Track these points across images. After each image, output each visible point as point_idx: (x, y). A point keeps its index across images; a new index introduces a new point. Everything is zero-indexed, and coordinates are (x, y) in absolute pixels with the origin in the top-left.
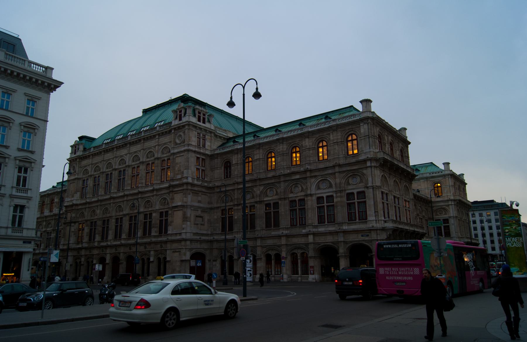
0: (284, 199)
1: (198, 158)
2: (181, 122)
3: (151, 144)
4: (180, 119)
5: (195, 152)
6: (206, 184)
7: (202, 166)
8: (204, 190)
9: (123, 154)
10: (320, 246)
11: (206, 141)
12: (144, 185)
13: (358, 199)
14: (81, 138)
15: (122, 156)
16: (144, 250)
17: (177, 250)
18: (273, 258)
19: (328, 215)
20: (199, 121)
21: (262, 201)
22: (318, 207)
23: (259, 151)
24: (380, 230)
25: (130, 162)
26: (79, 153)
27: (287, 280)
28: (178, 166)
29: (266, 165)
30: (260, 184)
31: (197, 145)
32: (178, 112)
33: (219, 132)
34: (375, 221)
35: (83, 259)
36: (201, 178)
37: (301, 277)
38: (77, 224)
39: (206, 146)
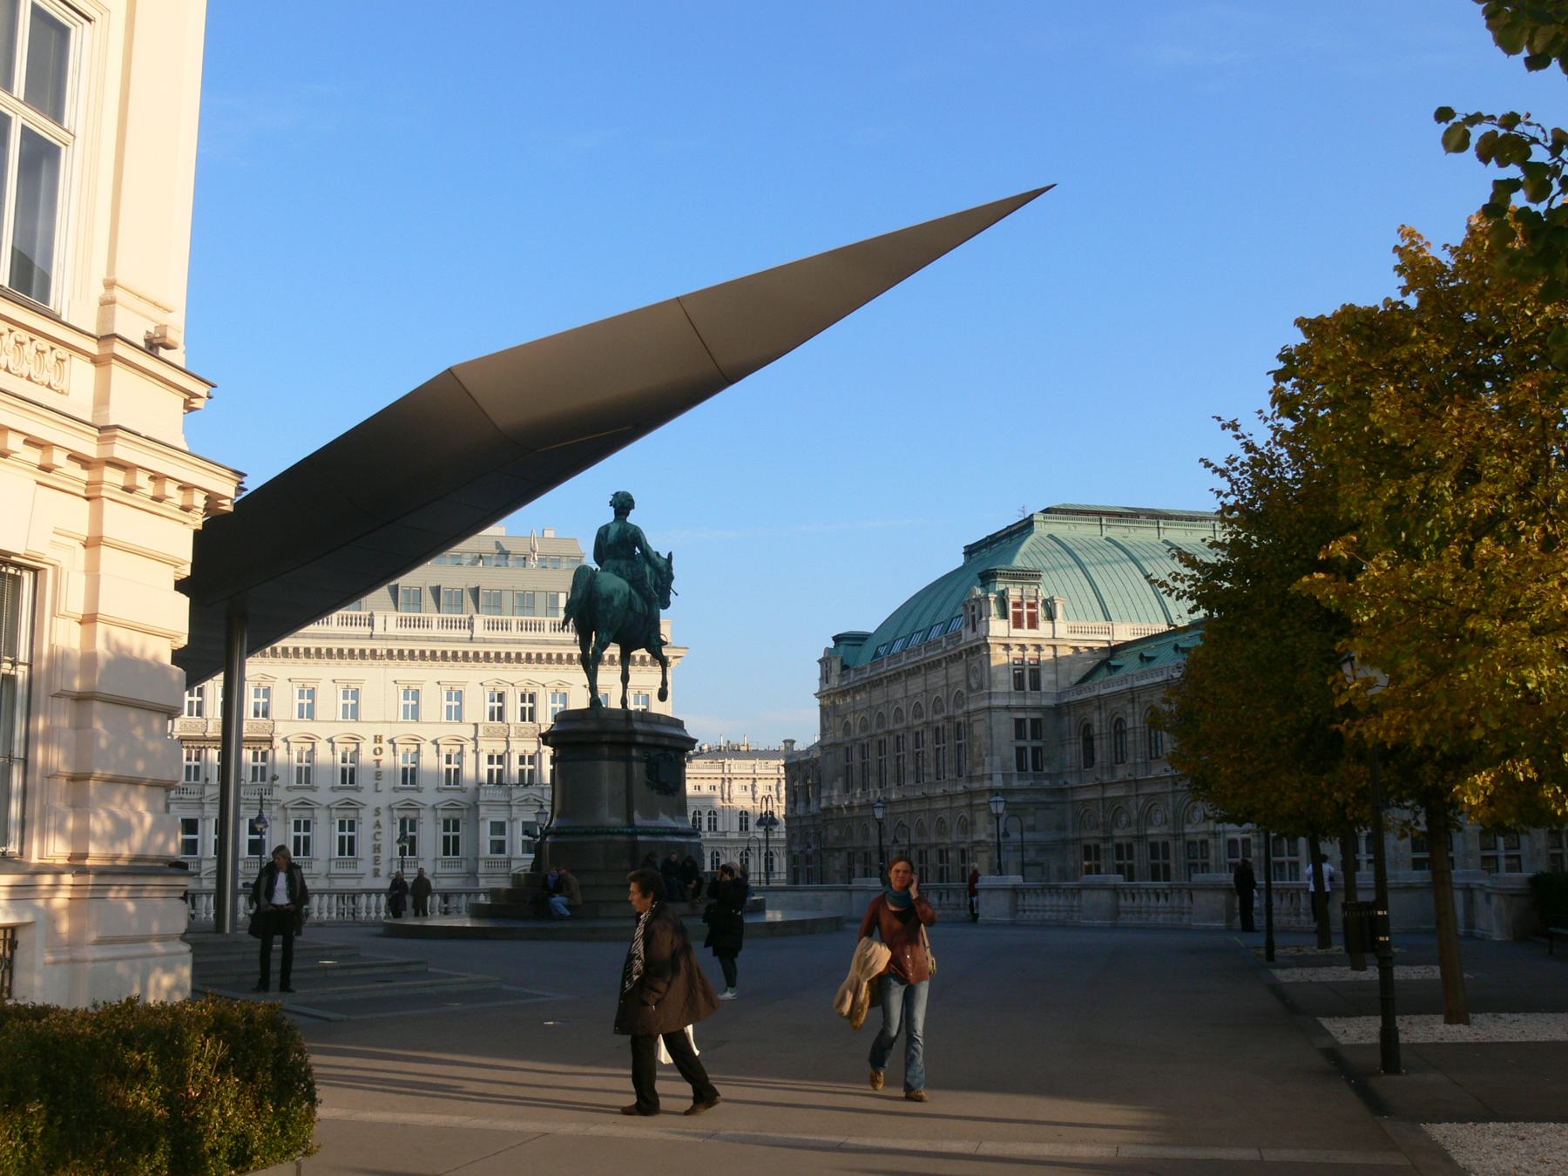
0: (1175, 836)
1: (1019, 723)
3: (937, 679)
4: (974, 630)
5: (1008, 708)
6: (1046, 783)
7: (1034, 737)
8: (1044, 798)
9: (898, 696)
11: (1042, 672)
12: (933, 779)
13: (1290, 855)
14: (837, 639)
15: (896, 702)
21: (1142, 837)
23: (1133, 708)
25: (910, 719)
26: (834, 682)
29: (1147, 744)
30: (1140, 792)
31: (1012, 689)
32: (970, 610)
33: (1085, 637)
36: (1030, 770)
38: (843, 853)
39: (1043, 685)
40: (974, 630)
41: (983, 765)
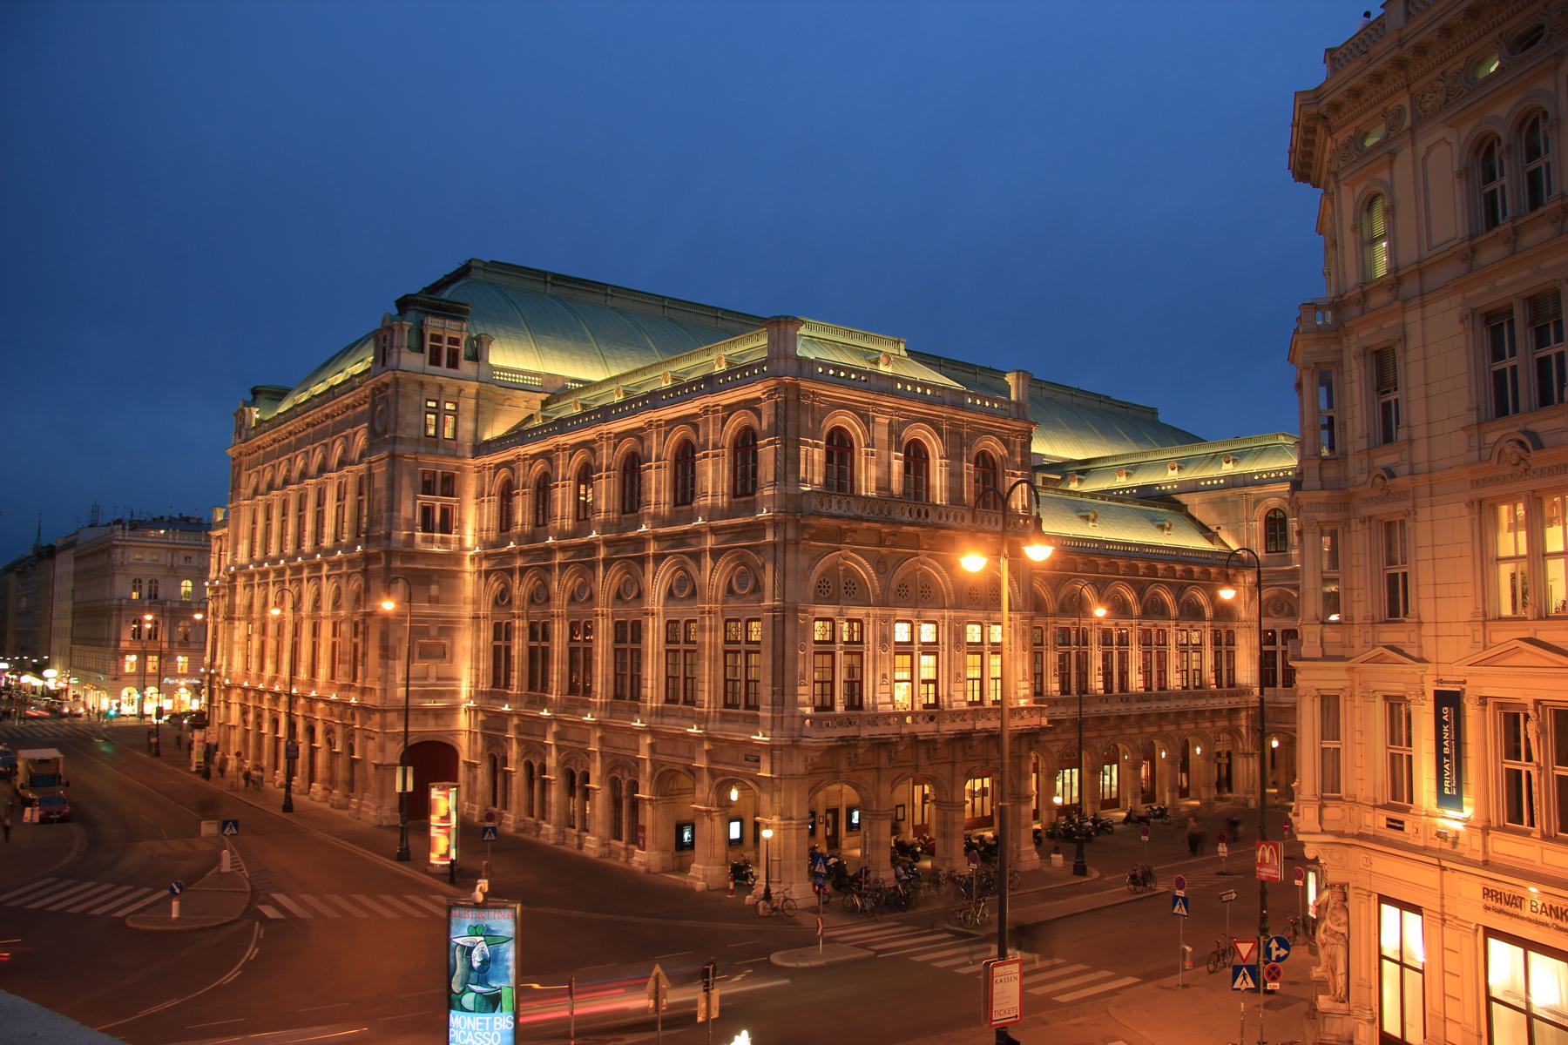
2: (385, 368)
4: (384, 364)
10: (663, 769)
16: (329, 719)
17: (372, 735)
18: (577, 784)
19: (686, 679)
20: (435, 360)
22: (667, 651)
24: (781, 748)
27: (595, 852)
28: (377, 497)
32: (381, 341)
34: (770, 721)
35: (251, 717)
37: (626, 849)
40: (384, 364)
41: (381, 524)
